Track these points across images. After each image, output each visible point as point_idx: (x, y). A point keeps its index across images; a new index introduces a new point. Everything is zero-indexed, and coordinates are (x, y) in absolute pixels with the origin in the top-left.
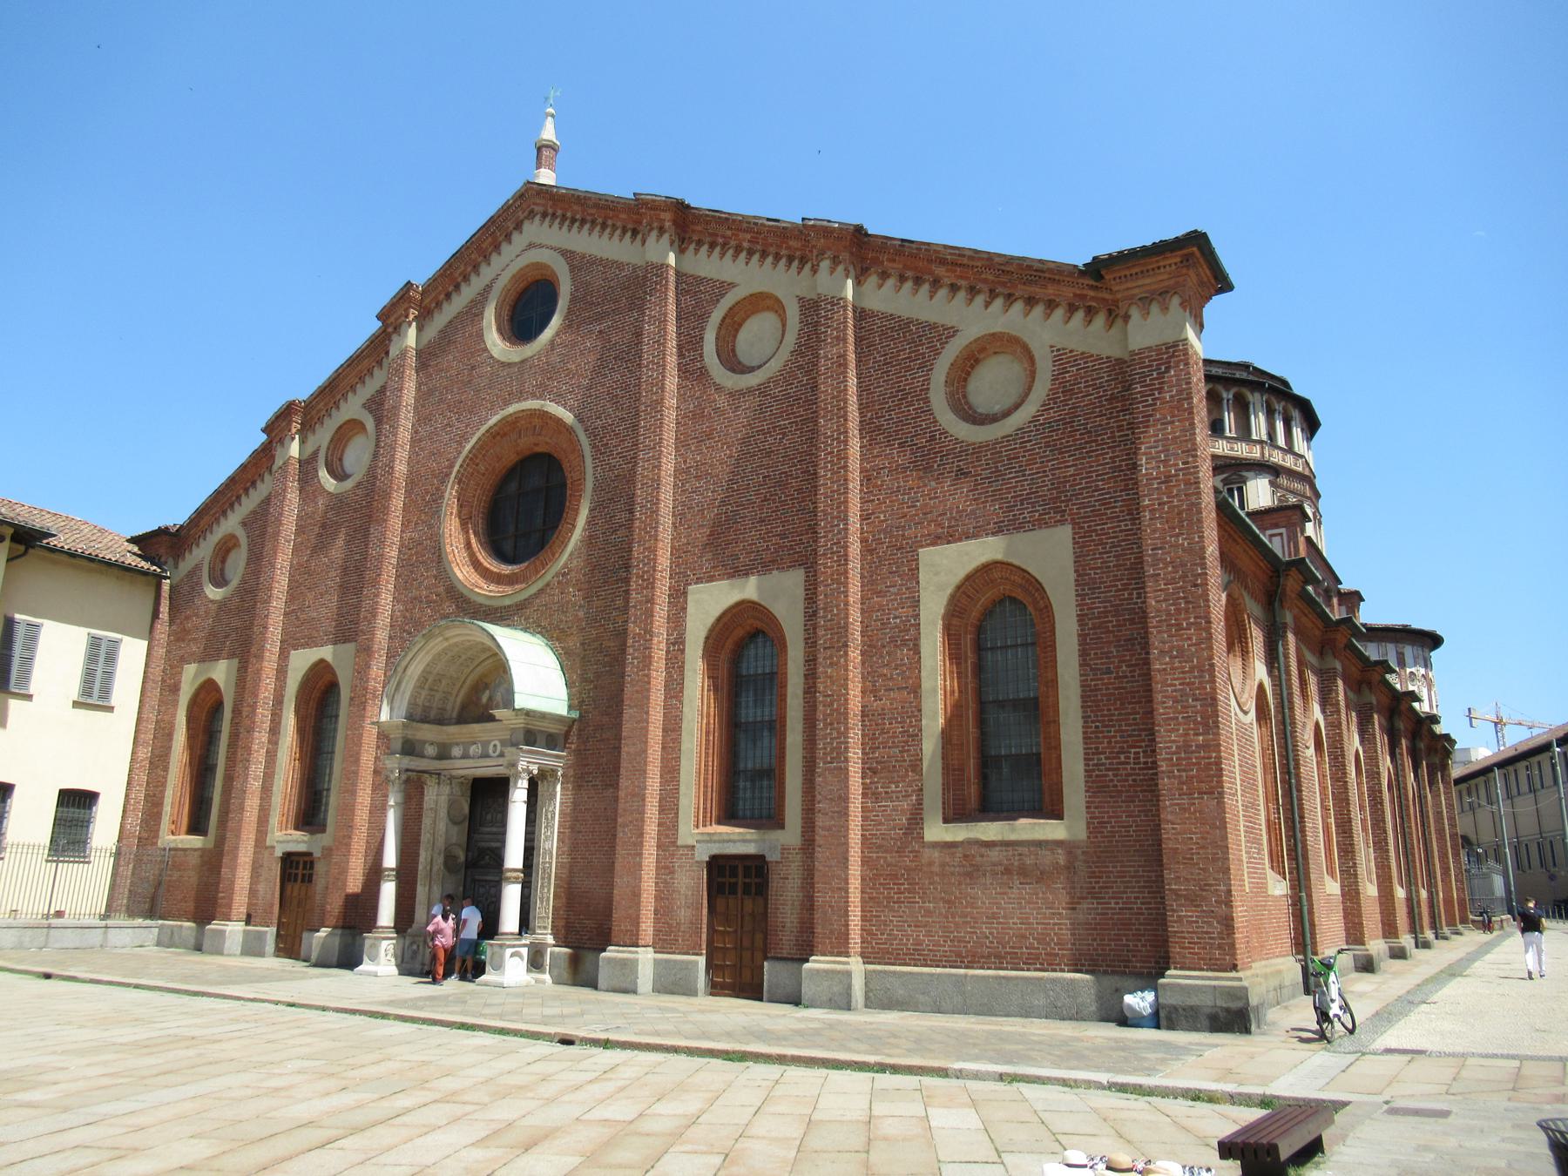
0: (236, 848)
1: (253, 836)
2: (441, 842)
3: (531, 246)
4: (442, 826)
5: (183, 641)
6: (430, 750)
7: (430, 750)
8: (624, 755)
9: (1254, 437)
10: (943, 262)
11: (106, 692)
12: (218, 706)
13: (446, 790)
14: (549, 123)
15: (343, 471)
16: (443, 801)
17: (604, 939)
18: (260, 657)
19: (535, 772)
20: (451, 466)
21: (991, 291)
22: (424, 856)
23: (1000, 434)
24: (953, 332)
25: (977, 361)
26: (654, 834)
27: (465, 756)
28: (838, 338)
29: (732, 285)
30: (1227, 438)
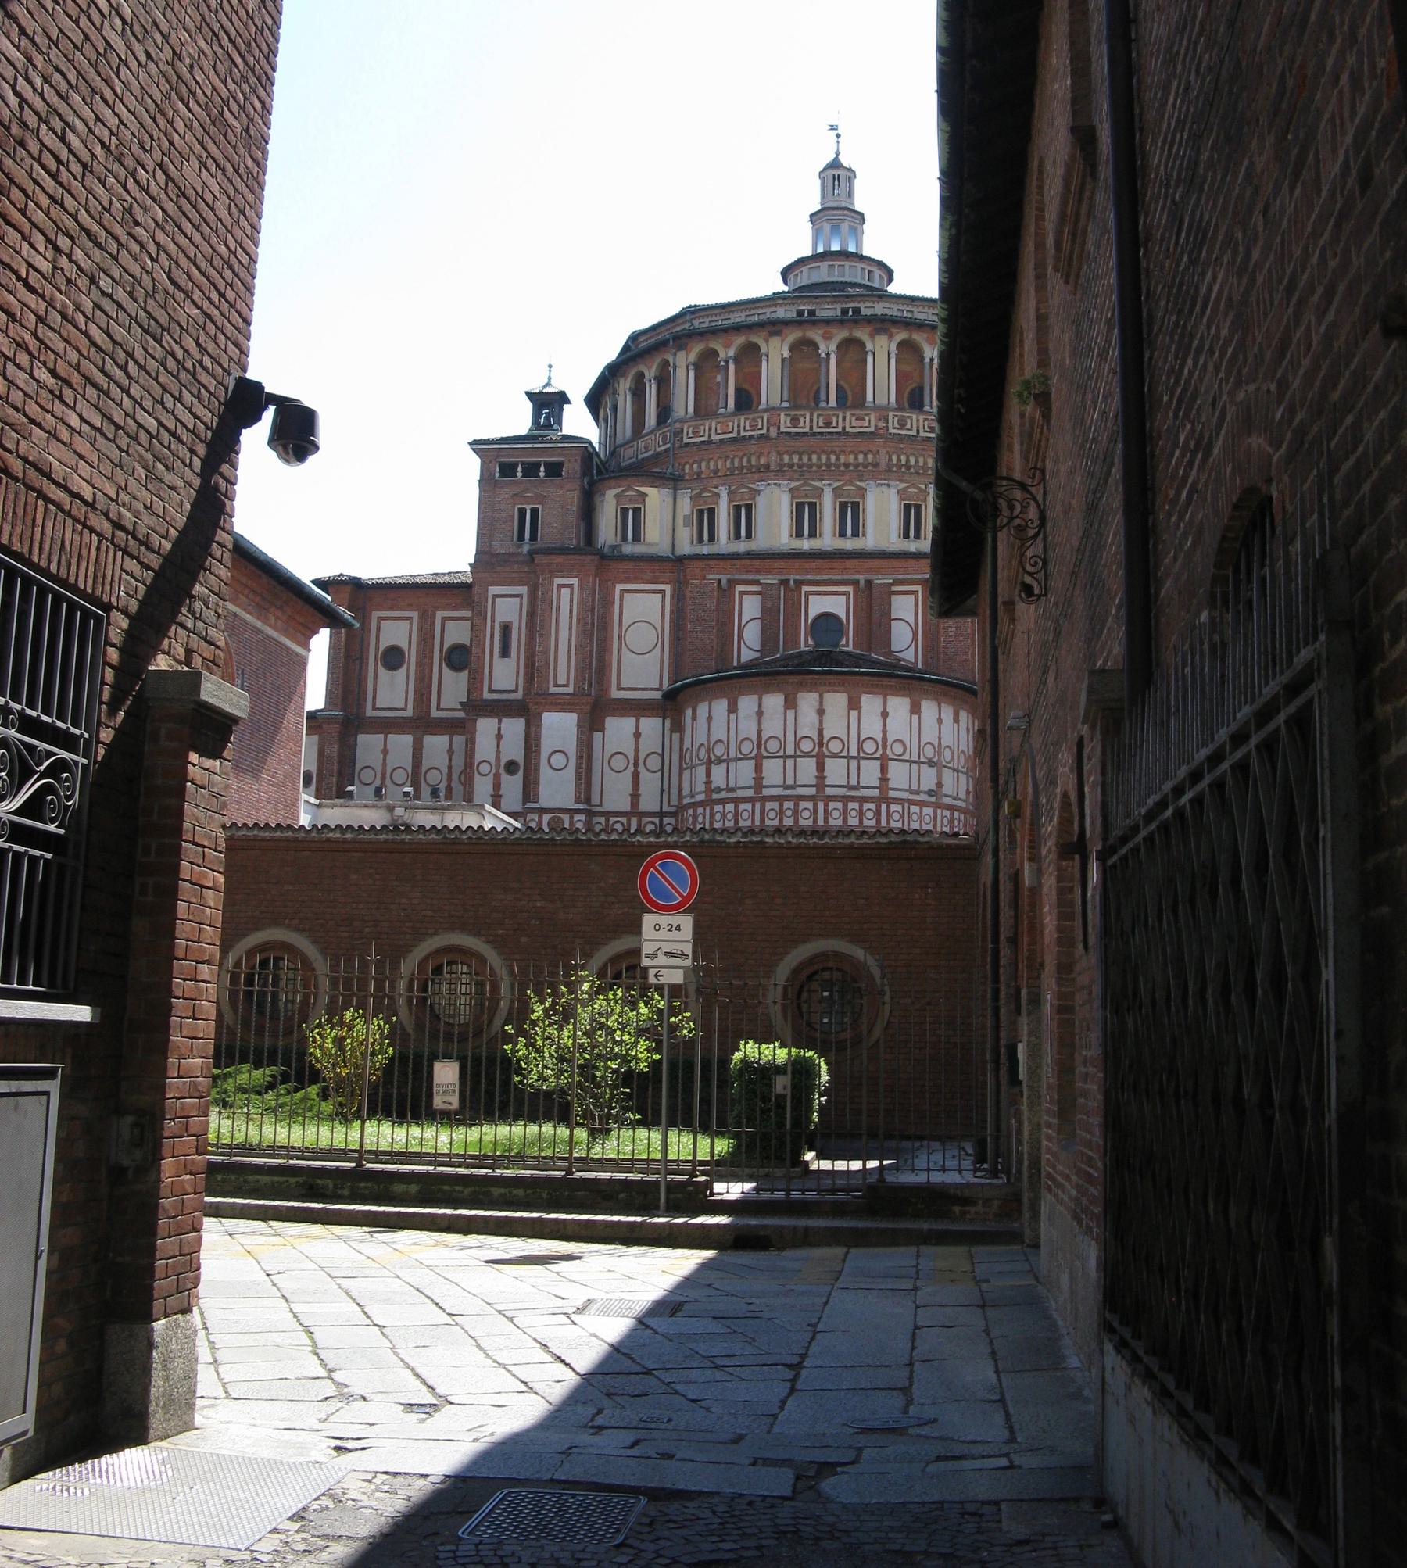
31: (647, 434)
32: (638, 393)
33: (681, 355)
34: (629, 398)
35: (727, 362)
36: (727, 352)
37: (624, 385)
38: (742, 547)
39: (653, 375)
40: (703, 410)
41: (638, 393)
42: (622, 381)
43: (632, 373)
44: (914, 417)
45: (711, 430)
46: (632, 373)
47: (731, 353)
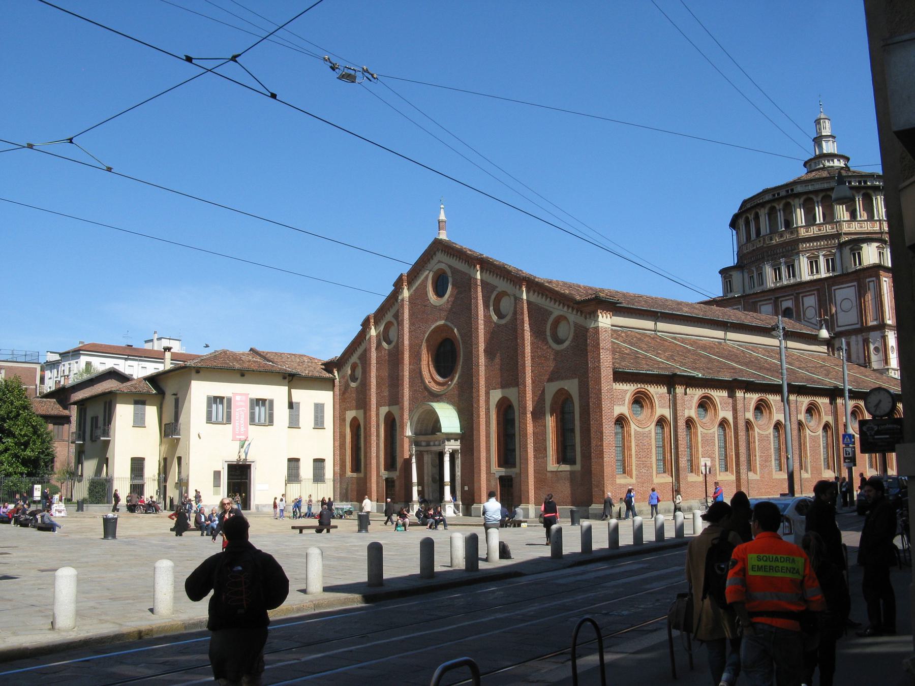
0: (371, 477)
1: (375, 473)
2: (430, 474)
3: (439, 262)
4: (430, 468)
5: (344, 402)
6: (424, 444)
7: (424, 444)
8: (474, 446)
9: (876, 218)
10: (547, 291)
11: (322, 423)
12: (359, 426)
13: (430, 456)
14: (442, 212)
15: (389, 339)
16: (430, 460)
17: (473, 502)
18: (370, 410)
19: (451, 451)
20: (422, 342)
21: (560, 301)
22: (426, 478)
23: (562, 348)
24: (551, 313)
25: (559, 322)
26: (485, 470)
27: (434, 445)
28: (521, 313)
29: (497, 287)
30: (857, 221)
31: (753, 241)
32: (747, 223)
33: (762, 210)
34: (744, 226)
35: (780, 211)
36: (779, 206)
37: (741, 222)
38: (792, 281)
39: (752, 217)
40: (773, 230)
41: (747, 223)
42: (740, 220)
43: (744, 216)
44: (853, 223)
45: (776, 240)
46: (744, 216)
47: (781, 206)
